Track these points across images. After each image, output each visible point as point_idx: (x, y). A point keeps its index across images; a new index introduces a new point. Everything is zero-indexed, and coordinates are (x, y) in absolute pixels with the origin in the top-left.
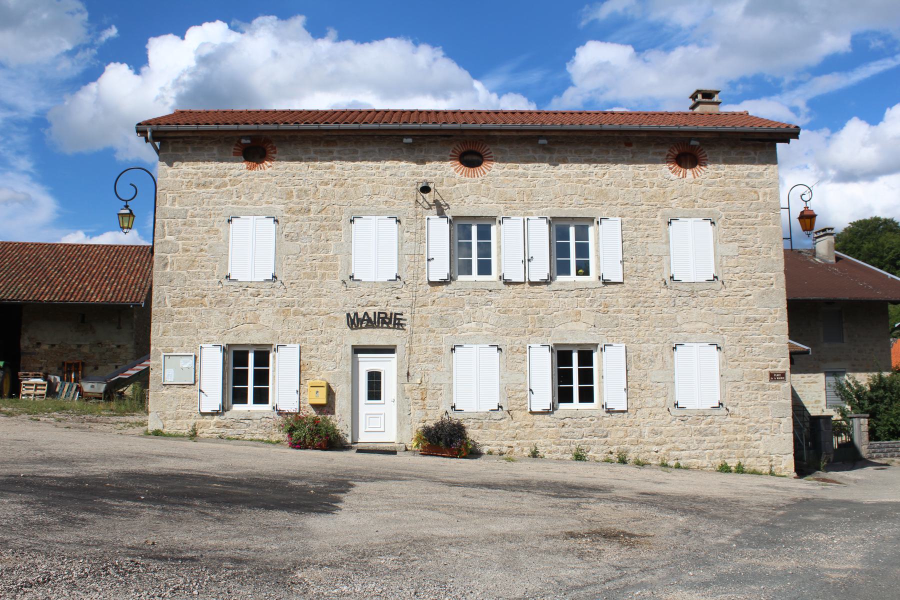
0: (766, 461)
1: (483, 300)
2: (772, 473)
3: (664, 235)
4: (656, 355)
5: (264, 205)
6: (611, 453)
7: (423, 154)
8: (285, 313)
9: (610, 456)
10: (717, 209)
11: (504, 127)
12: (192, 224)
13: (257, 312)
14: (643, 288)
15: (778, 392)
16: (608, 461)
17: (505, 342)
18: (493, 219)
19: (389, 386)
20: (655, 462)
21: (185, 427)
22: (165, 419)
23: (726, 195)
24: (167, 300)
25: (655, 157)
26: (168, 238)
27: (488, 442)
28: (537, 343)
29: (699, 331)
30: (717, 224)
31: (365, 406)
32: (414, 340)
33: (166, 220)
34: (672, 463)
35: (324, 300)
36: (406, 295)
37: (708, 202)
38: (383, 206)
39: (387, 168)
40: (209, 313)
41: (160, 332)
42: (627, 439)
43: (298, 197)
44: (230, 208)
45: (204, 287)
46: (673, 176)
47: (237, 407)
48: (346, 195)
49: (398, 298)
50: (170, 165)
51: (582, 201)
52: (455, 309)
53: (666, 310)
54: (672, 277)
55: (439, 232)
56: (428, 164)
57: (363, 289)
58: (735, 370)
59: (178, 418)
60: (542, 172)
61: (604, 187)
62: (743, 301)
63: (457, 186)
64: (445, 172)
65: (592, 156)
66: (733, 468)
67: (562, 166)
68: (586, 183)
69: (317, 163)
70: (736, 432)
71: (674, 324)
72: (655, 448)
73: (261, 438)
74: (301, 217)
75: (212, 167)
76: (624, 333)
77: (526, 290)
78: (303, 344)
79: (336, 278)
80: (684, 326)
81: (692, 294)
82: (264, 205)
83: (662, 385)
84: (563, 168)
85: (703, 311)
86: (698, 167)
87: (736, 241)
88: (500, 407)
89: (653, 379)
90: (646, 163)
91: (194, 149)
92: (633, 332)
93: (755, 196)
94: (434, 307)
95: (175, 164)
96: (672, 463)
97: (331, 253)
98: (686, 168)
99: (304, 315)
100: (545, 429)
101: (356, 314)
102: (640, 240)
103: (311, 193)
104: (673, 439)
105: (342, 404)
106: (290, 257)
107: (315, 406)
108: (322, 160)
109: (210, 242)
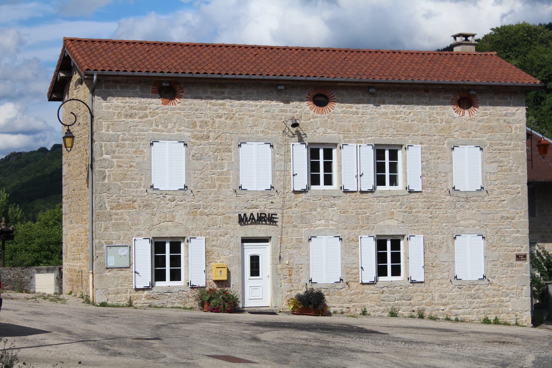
0: (513, 316)
1: (329, 204)
2: (517, 324)
3: (449, 158)
4: (443, 243)
5: (176, 133)
6: (414, 311)
7: (287, 96)
8: (194, 214)
9: (413, 313)
10: (484, 139)
11: (348, 80)
12: (123, 146)
13: (174, 213)
14: (435, 195)
15: (521, 268)
16: (412, 317)
17: (345, 233)
18: (336, 145)
19: (265, 266)
20: (441, 317)
21: (123, 299)
22: (109, 294)
23: (491, 129)
24: (106, 205)
25: (444, 101)
26: (105, 156)
27: (334, 305)
28: (365, 234)
29: (471, 226)
30: (484, 150)
31: (250, 281)
32: (284, 233)
33: (103, 143)
34: (453, 318)
35: (220, 204)
36: (278, 200)
37: (479, 134)
38: (261, 135)
39: (263, 106)
40: (138, 214)
41: (103, 229)
42: (424, 301)
43: (201, 126)
44: (150, 133)
45: (134, 194)
46: (456, 115)
47: (159, 284)
48: (234, 126)
49: (272, 203)
50: (105, 99)
51: (395, 133)
52: (311, 210)
53: (449, 211)
54: (454, 188)
55: (300, 155)
56: (291, 104)
57: (248, 196)
58: (494, 253)
59: (118, 293)
60: (368, 111)
61: (410, 122)
62: (500, 205)
63: (311, 120)
64: (303, 109)
65: (403, 99)
66: (492, 321)
67: (382, 106)
68: (398, 119)
69: (214, 101)
70: (494, 296)
71: (455, 221)
72: (442, 308)
73: (179, 306)
74: (203, 142)
75: (136, 101)
76: (422, 227)
77: (358, 196)
78: (207, 237)
79: (229, 188)
80: (461, 222)
81: (467, 199)
82: (176, 133)
83: (446, 264)
84: (383, 108)
85: (474, 211)
86: (472, 108)
87: (496, 162)
88: (341, 280)
89: (441, 260)
90: (438, 105)
91: (122, 87)
92: (428, 227)
93: (510, 130)
94: (297, 209)
95: (108, 98)
96: (453, 318)
97: (225, 169)
98: (465, 109)
99: (207, 215)
100: (370, 295)
101: (245, 215)
102: (433, 161)
103: (210, 124)
104: (454, 301)
105: (235, 280)
106: (197, 172)
107: (217, 282)
108: (217, 99)
109: (137, 160)
